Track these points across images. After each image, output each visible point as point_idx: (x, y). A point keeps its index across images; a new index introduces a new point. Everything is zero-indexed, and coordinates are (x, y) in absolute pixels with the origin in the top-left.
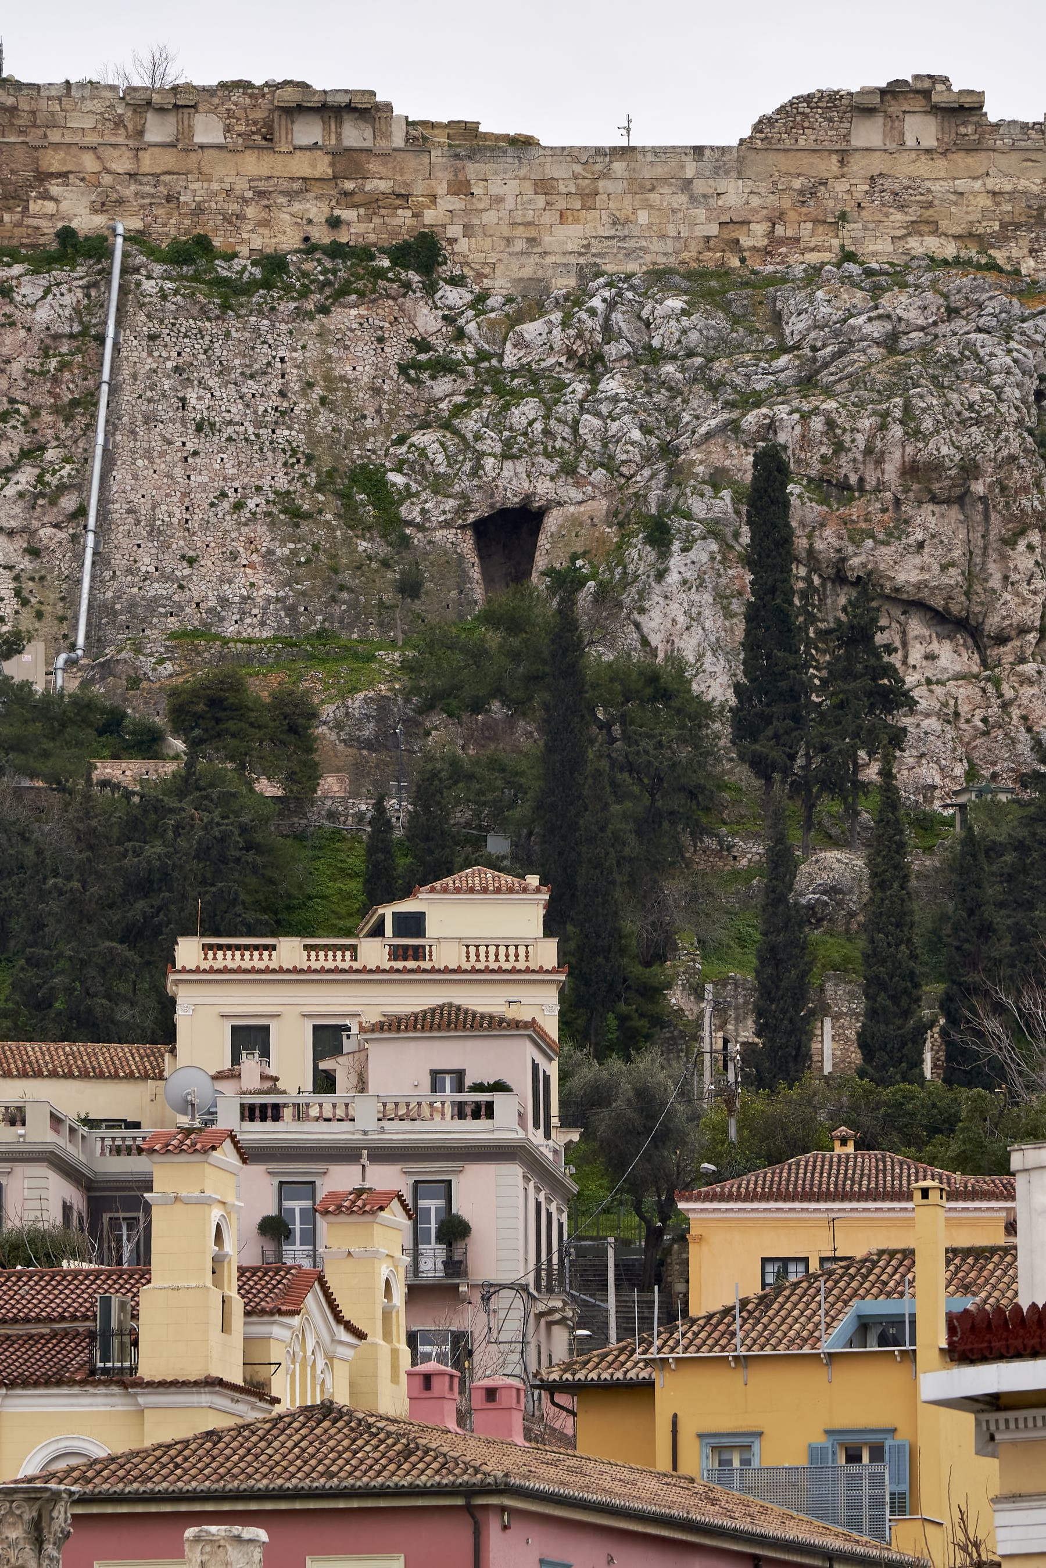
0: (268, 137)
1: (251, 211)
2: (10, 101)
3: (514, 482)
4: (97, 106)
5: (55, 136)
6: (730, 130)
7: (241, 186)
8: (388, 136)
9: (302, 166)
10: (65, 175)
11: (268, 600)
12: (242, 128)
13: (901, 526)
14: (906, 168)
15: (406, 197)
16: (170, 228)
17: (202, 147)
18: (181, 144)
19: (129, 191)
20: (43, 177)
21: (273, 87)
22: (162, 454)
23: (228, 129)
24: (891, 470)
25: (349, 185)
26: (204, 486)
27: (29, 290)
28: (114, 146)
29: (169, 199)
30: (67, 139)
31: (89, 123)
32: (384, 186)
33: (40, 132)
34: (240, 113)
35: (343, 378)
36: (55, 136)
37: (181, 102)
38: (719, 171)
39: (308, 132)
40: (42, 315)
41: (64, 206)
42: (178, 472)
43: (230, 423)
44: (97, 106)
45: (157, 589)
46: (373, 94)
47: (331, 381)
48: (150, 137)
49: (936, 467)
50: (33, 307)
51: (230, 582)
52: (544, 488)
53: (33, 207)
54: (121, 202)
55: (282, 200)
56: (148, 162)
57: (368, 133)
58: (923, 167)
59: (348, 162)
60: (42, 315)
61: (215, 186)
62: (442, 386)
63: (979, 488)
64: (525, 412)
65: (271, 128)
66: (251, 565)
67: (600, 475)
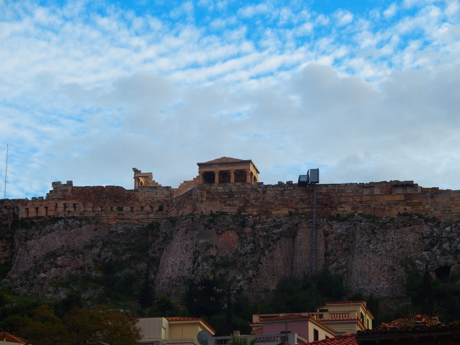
0: (390, 193)
1: (387, 208)
2: (334, 188)
3: (442, 261)
4: (353, 188)
5: (343, 194)
8: (416, 190)
9: (397, 198)
10: (345, 202)
11: (387, 288)
12: (384, 191)
15: (421, 203)
16: (368, 212)
17: (376, 195)
19: (359, 205)
20: (341, 203)
21: (391, 181)
22: (364, 258)
23: (381, 191)
25: (409, 201)
26: (373, 265)
27: (336, 226)
28: (356, 196)
29: (369, 206)
30: (346, 195)
31: (351, 191)
32: (416, 201)
33: (340, 194)
34: (384, 188)
35: (406, 241)
36: (343, 194)
37: (371, 186)
40: (339, 231)
41: (345, 209)
42: (368, 262)
43: (380, 251)
44: (353, 188)
45: (362, 287)
46: (413, 181)
47: (403, 242)
48: (364, 194)
50: (337, 229)
51: (378, 284)
52: (450, 261)
53: (339, 209)
54: (358, 207)
55: (394, 205)
56: (364, 199)
57: (413, 190)
59: (408, 197)
60: (339, 231)
61: (378, 203)
65: (391, 191)
66: (383, 281)
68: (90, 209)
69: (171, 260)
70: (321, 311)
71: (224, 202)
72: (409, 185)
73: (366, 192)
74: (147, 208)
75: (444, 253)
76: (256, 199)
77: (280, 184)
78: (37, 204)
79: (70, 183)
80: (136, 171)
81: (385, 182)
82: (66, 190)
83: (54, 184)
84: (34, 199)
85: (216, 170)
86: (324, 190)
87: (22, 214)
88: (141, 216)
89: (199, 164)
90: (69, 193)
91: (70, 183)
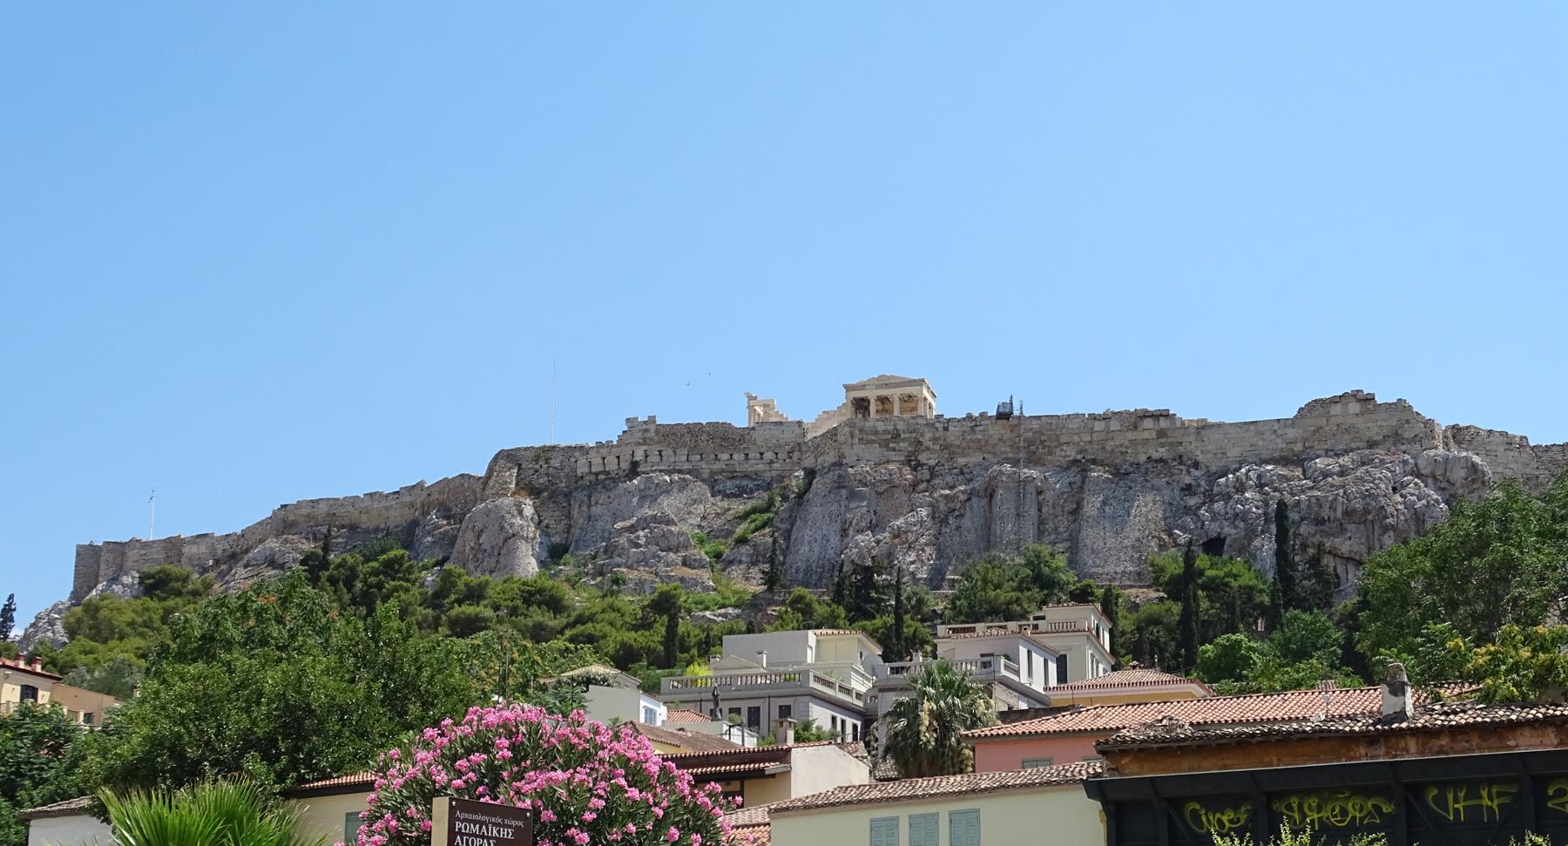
0: (1136, 428)
3: (1213, 529)
6: (1291, 413)
7: (1126, 443)
9: (1146, 435)
13: (1342, 530)
14: (1349, 421)
18: (1107, 431)
24: (1339, 513)
38: (1286, 426)
39: (1148, 423)
49: (1354, 511)
58: (1356, 420)
59: (1162, 433)
62: (1192, 502)
63: (1370, 517)
64: (1218, 506)
67: (1242, 525)
68: (684, 458)
69: (808, 534)
70: (1036, 618)
71: (885, 444)
72: (1164, 415)
73: (1099, 426)
74: (769, 455)
75: (1215, 517)
76: (935, 440)
77: (969, 417)
78: (604, 451)
79: (652, 419)
80: (751, 398)
81: (1127, 412)
82: (646, 431)
83: (628, 420)
84: (600, 445)
85: (872, 394)
86: (1035, 425)
87: (582, 469)
88: (761, 467)
89: (845, 387)
90: (652, 434)
91: (652, 419)
